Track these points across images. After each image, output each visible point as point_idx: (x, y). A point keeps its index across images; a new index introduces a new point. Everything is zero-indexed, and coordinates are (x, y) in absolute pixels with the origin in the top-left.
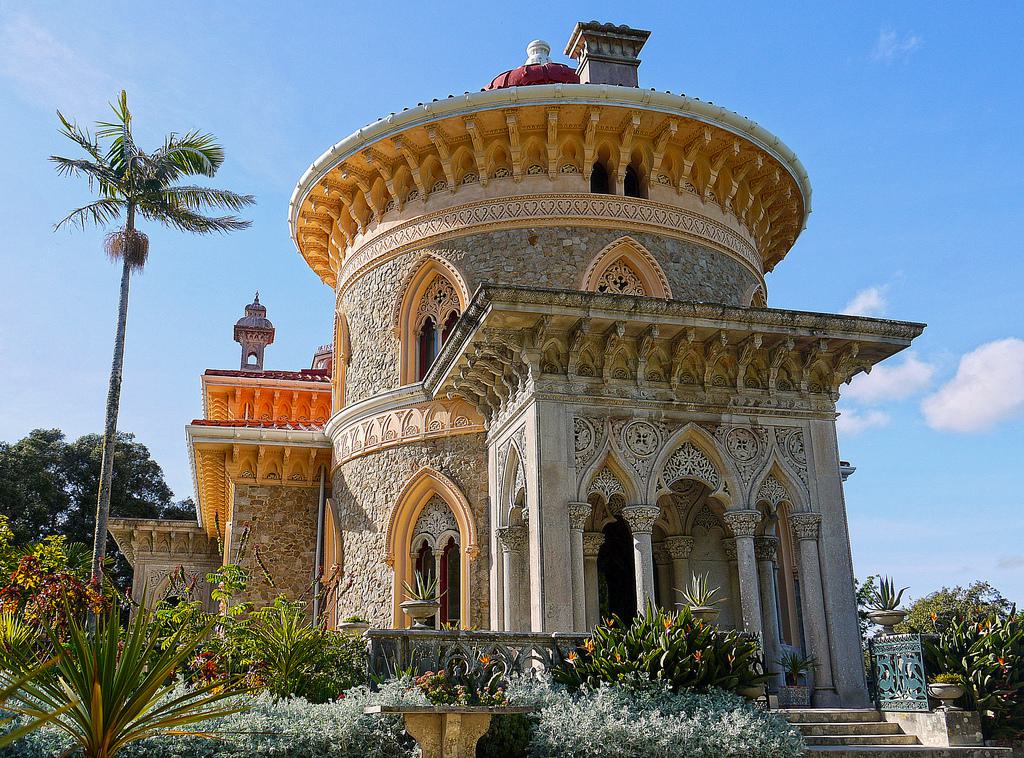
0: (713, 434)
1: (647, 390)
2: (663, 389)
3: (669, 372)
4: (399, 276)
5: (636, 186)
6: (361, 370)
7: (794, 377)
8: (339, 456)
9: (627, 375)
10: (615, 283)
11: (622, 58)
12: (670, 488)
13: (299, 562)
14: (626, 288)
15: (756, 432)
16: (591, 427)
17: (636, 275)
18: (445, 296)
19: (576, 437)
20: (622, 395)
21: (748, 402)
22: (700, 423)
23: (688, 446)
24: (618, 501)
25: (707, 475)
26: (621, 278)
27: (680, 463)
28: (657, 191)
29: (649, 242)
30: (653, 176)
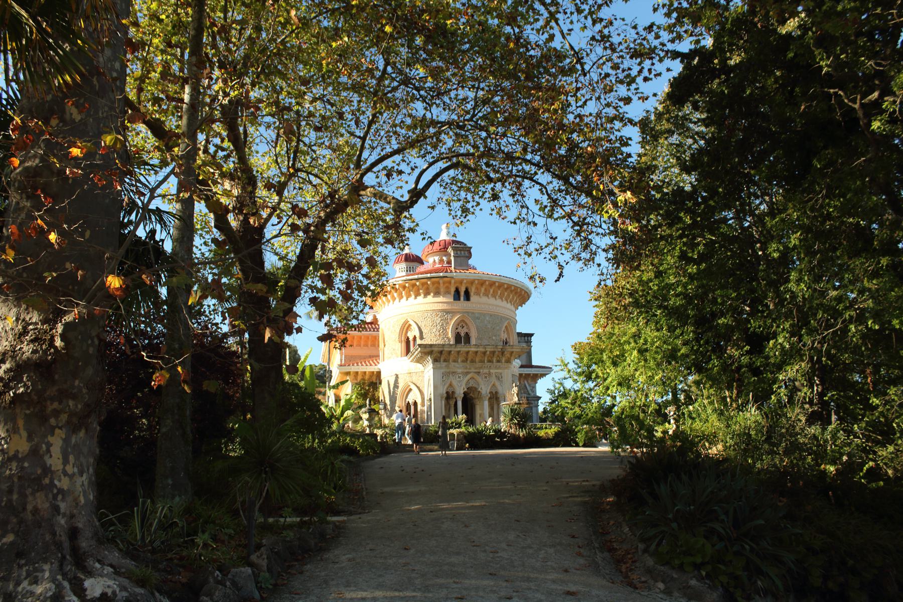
1: (461, 364)
3: (467, 360)
5: (467, 297)
15: (490, 374)
17: (467, 324)
20: (454, 366)
22: (475, 372)
23: (472, 378)
24: (453, 393)
28: (473, 298)
30: (472, 294)
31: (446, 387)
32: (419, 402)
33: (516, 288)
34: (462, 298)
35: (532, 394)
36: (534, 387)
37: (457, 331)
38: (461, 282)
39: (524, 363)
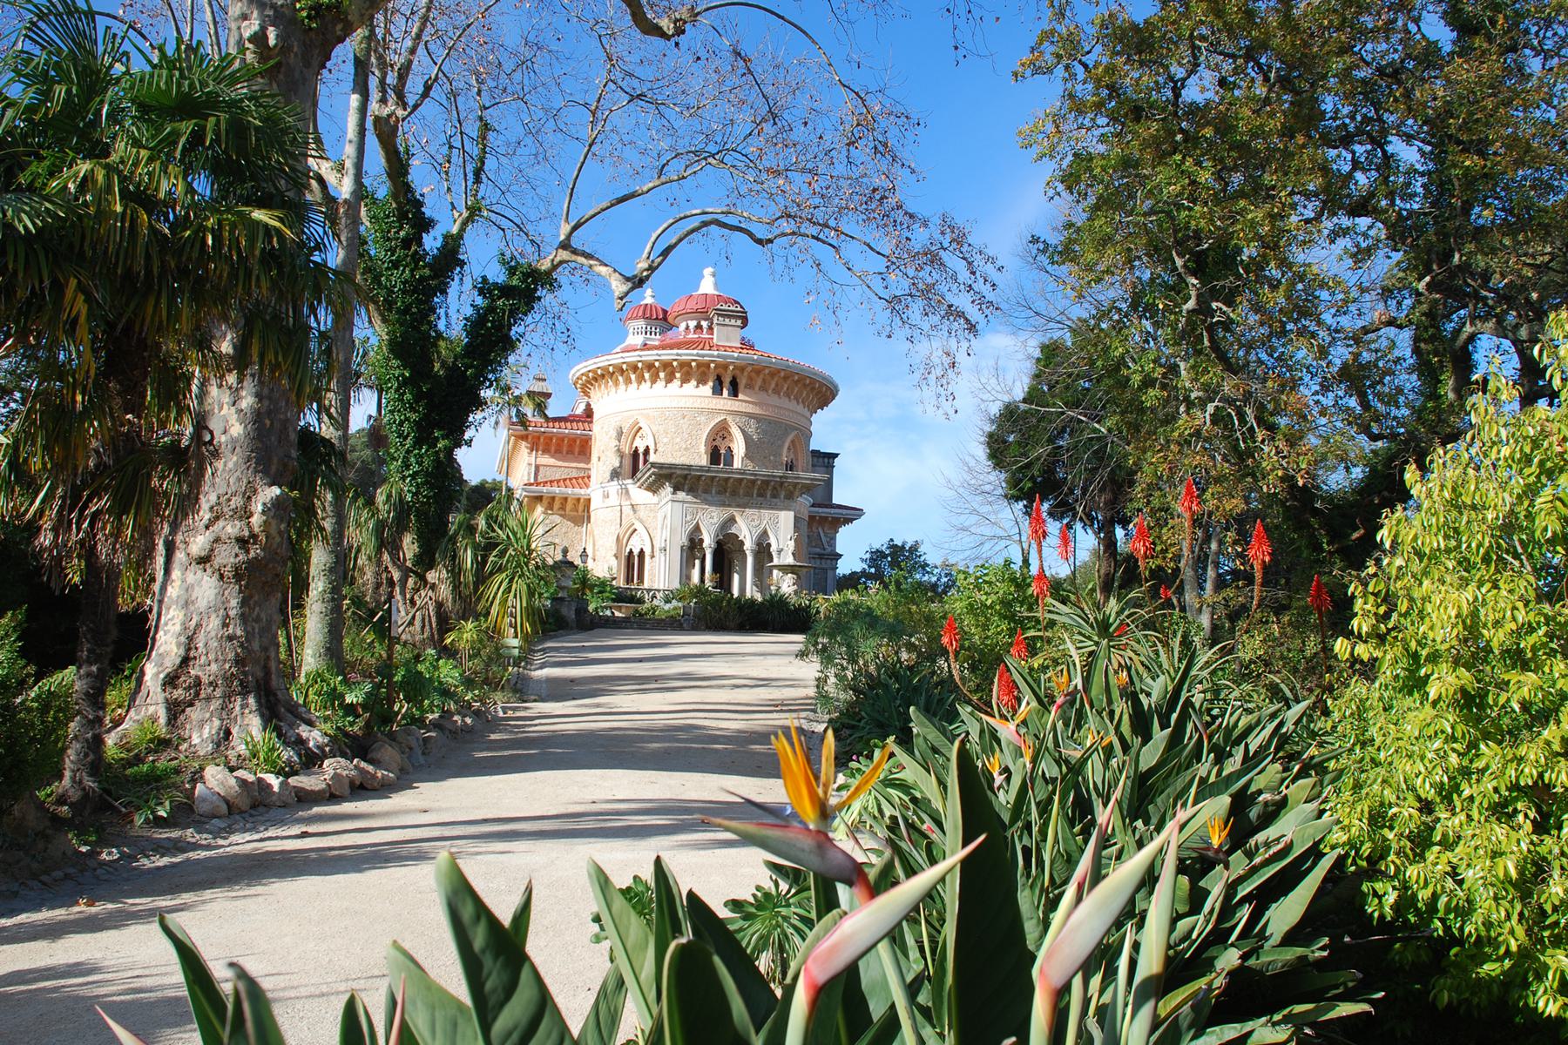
2: (722, 498)
32: (648, 552)
33: (813, 381)
34: (725, 392)
35: (829, 550)
36: (834, 539)
38: (725, 367)
39: (819, 501)
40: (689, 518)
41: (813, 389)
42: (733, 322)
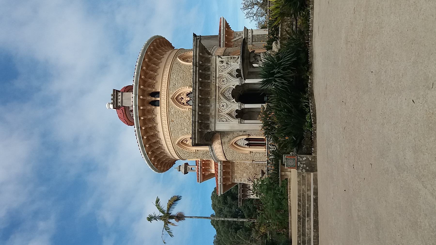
0: (221, 88)
4: (182, 150)
6: (205, 157)
7: (207, 67)
8: (225, 160)
9: (208, 110)
10: (182, 100)
11: (121, 96)
12: (234, 99)
13: (250, 166)
14: (183, 98)
16: (221, 118)
17: (180, 95)
18: (186, 140)
19: (223, 121)
21: (213, 79)
24: (237, 111)
25: (230, 90)
26: (181, 99)
27: (228, 96)
29: (171, 92)
30: (154, 90)
31: (231, 119)
32: (246, 137)
37: (185, 103)
39: (218, 43)
40: (225, 120)
41: (155, 50)
42: (120, 97)
